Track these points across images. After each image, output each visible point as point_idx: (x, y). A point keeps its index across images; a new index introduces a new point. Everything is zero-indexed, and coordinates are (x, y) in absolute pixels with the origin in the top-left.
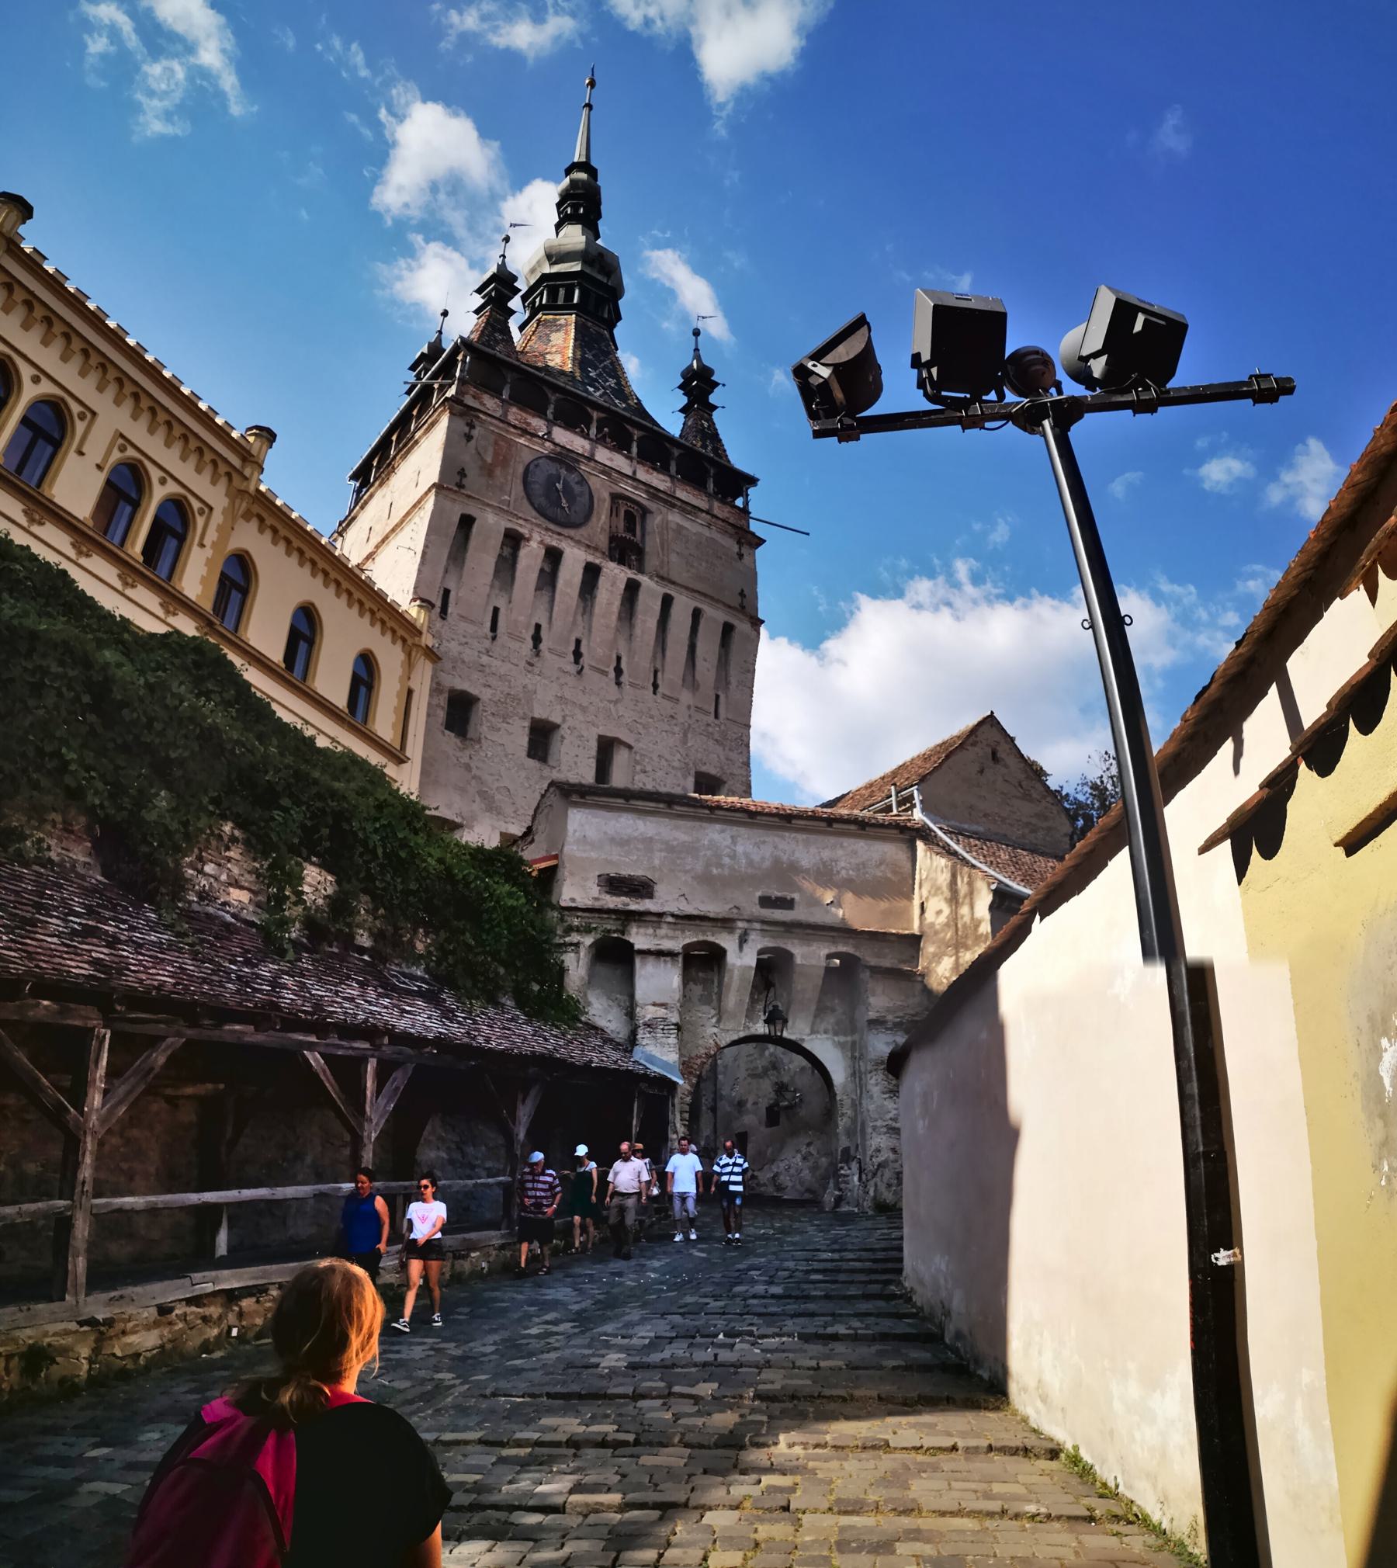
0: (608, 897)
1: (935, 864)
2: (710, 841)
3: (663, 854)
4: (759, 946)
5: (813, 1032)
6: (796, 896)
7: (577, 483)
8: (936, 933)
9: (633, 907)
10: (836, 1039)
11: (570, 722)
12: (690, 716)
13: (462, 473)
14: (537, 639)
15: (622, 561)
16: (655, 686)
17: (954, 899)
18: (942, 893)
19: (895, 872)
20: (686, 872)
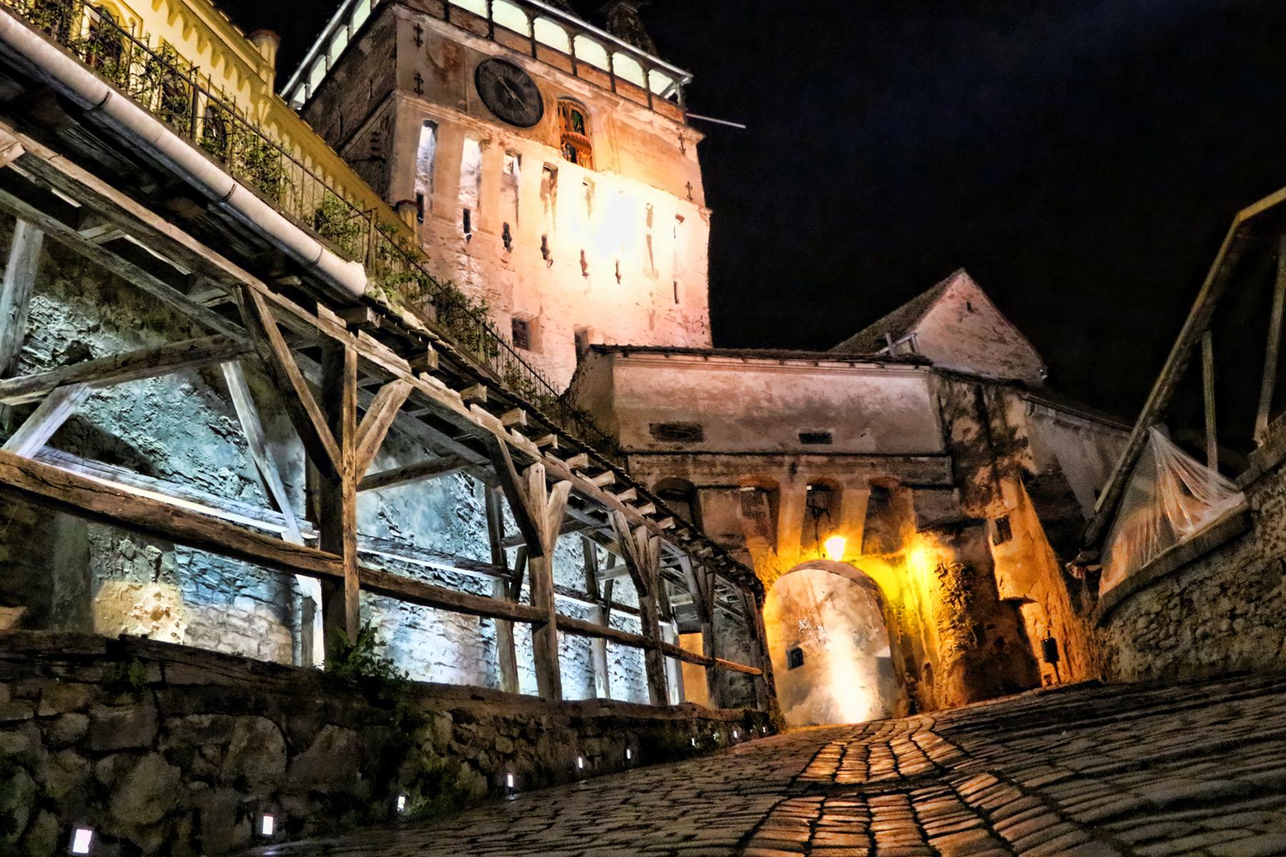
0: (661, 443)
1: (956, 390)
2: (748, 387)
3: (706, 402)
4: (807, 476)
5: (864, 551)
6: (831, 430)
7: (525, 84)
8: (966, 449)
9: (689, 449)
10: (885, 556)
11: (547, 313)
12: (653, 303)
13: (418, 78)
14: (507, 238)
15: (574, 160)
16: (618, 276)
17: (983, 416)
18: (968, 414)
19: (915, 404)
20: (730, 416)
